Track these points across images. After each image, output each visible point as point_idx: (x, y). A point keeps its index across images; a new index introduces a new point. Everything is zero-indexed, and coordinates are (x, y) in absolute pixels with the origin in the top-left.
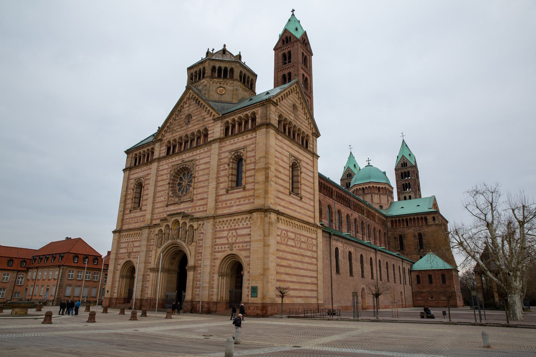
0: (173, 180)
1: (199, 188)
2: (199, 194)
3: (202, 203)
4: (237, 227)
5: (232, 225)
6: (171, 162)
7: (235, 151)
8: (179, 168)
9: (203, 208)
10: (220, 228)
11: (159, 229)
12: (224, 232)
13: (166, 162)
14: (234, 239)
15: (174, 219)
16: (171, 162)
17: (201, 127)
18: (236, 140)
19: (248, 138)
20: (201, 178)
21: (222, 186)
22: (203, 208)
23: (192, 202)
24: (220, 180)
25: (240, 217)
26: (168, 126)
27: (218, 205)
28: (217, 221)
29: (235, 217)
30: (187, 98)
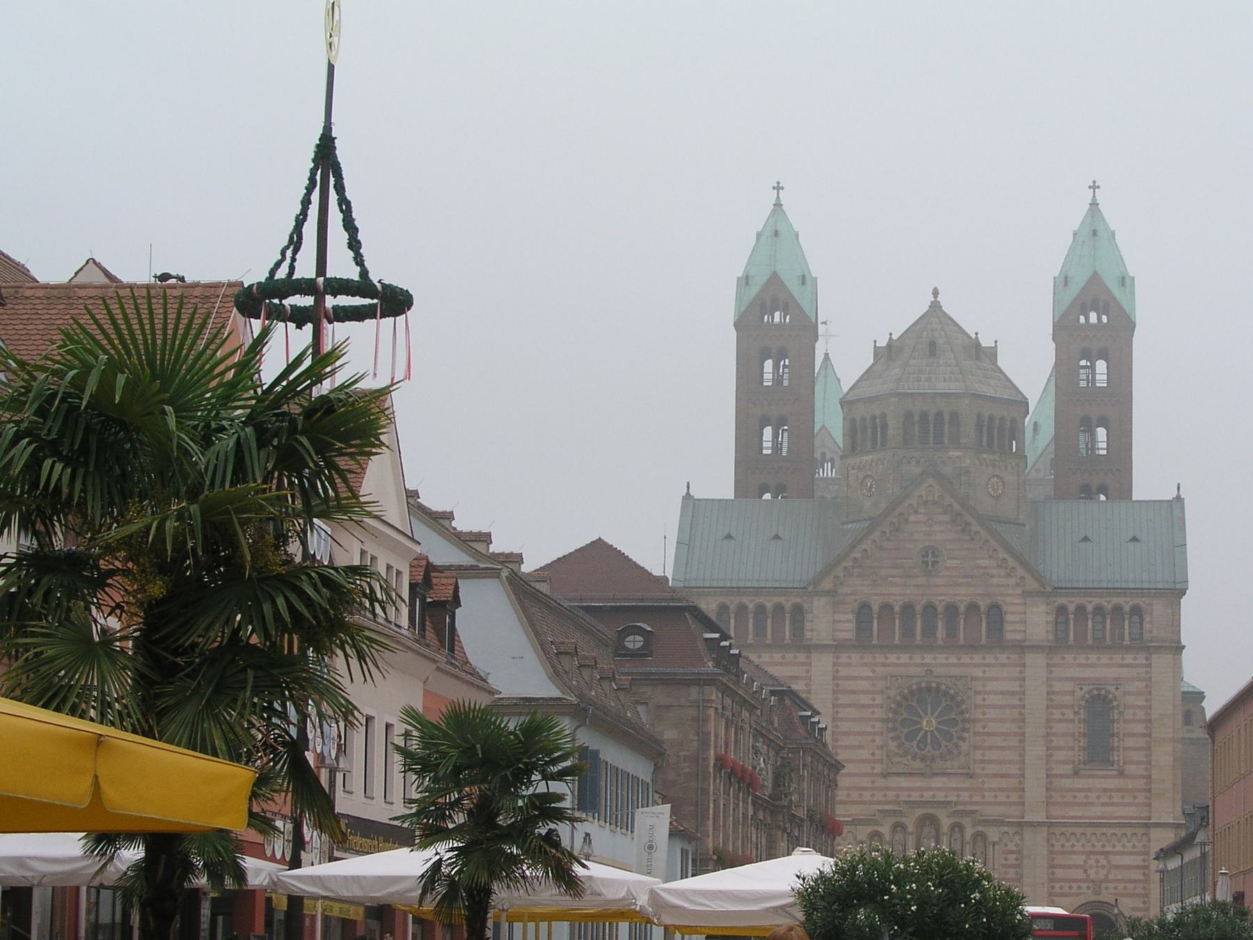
0: (896, 712)
1: (990, 748)
2: (990, 762)
3: (1005, 786)
4: (1108, 849)
5: (1095, 843)
6: (884, 665)
7: (1094, 685)
8: (914, 687)
9: (1008, 797)
10: (1063, 846)
11: (870, 829)
12: (1074, 857)
13: (862, 658)
14: (1103, 872)
15: (920, 812)
16: (884, 665)
17: (979, 595)
18: (1093, 658)
19: (1125, 662)
20: (992, 727)
21: (1059, 755)
22: (1008, 797)
23: (971, 777)
24: (1053, 741)
25: (1119, 831)
26: (855, 559)
27: (1051, 797)
28: (1057, 831)
29: (1104, 830)
30: (921, 496)
